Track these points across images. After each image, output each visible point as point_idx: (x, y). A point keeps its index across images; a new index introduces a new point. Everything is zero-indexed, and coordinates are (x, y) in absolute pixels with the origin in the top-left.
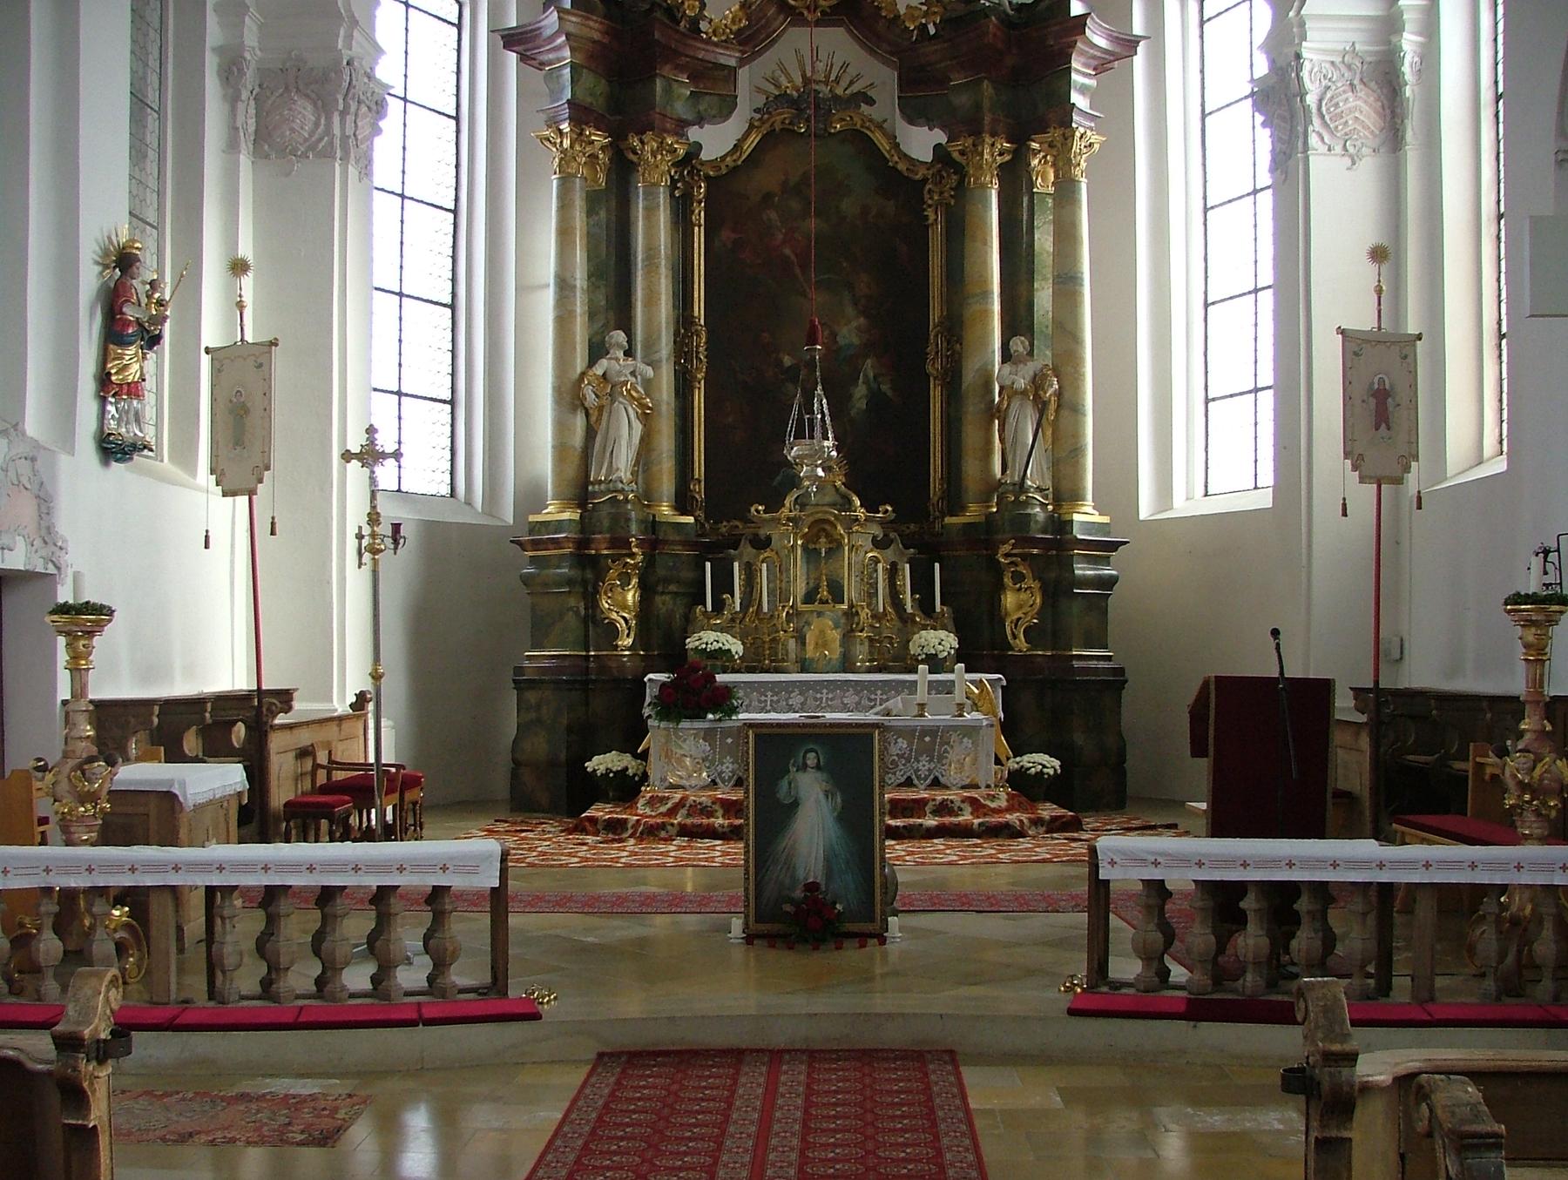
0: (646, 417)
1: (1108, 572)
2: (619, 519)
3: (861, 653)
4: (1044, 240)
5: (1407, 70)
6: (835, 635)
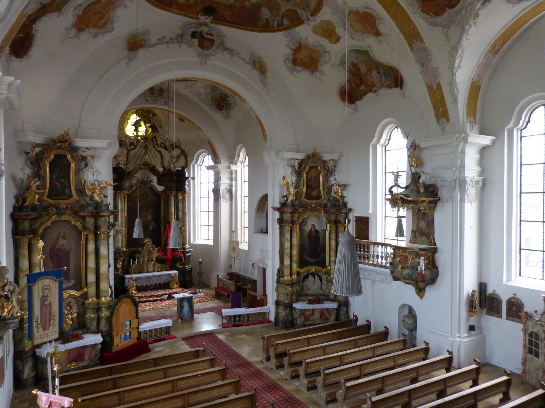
0: (122, 236)
1: (190, 254)
2: (119, 253)
3: (156, 269)
4: (180, 206)
5: (233, 192)
6: (152, 267)
